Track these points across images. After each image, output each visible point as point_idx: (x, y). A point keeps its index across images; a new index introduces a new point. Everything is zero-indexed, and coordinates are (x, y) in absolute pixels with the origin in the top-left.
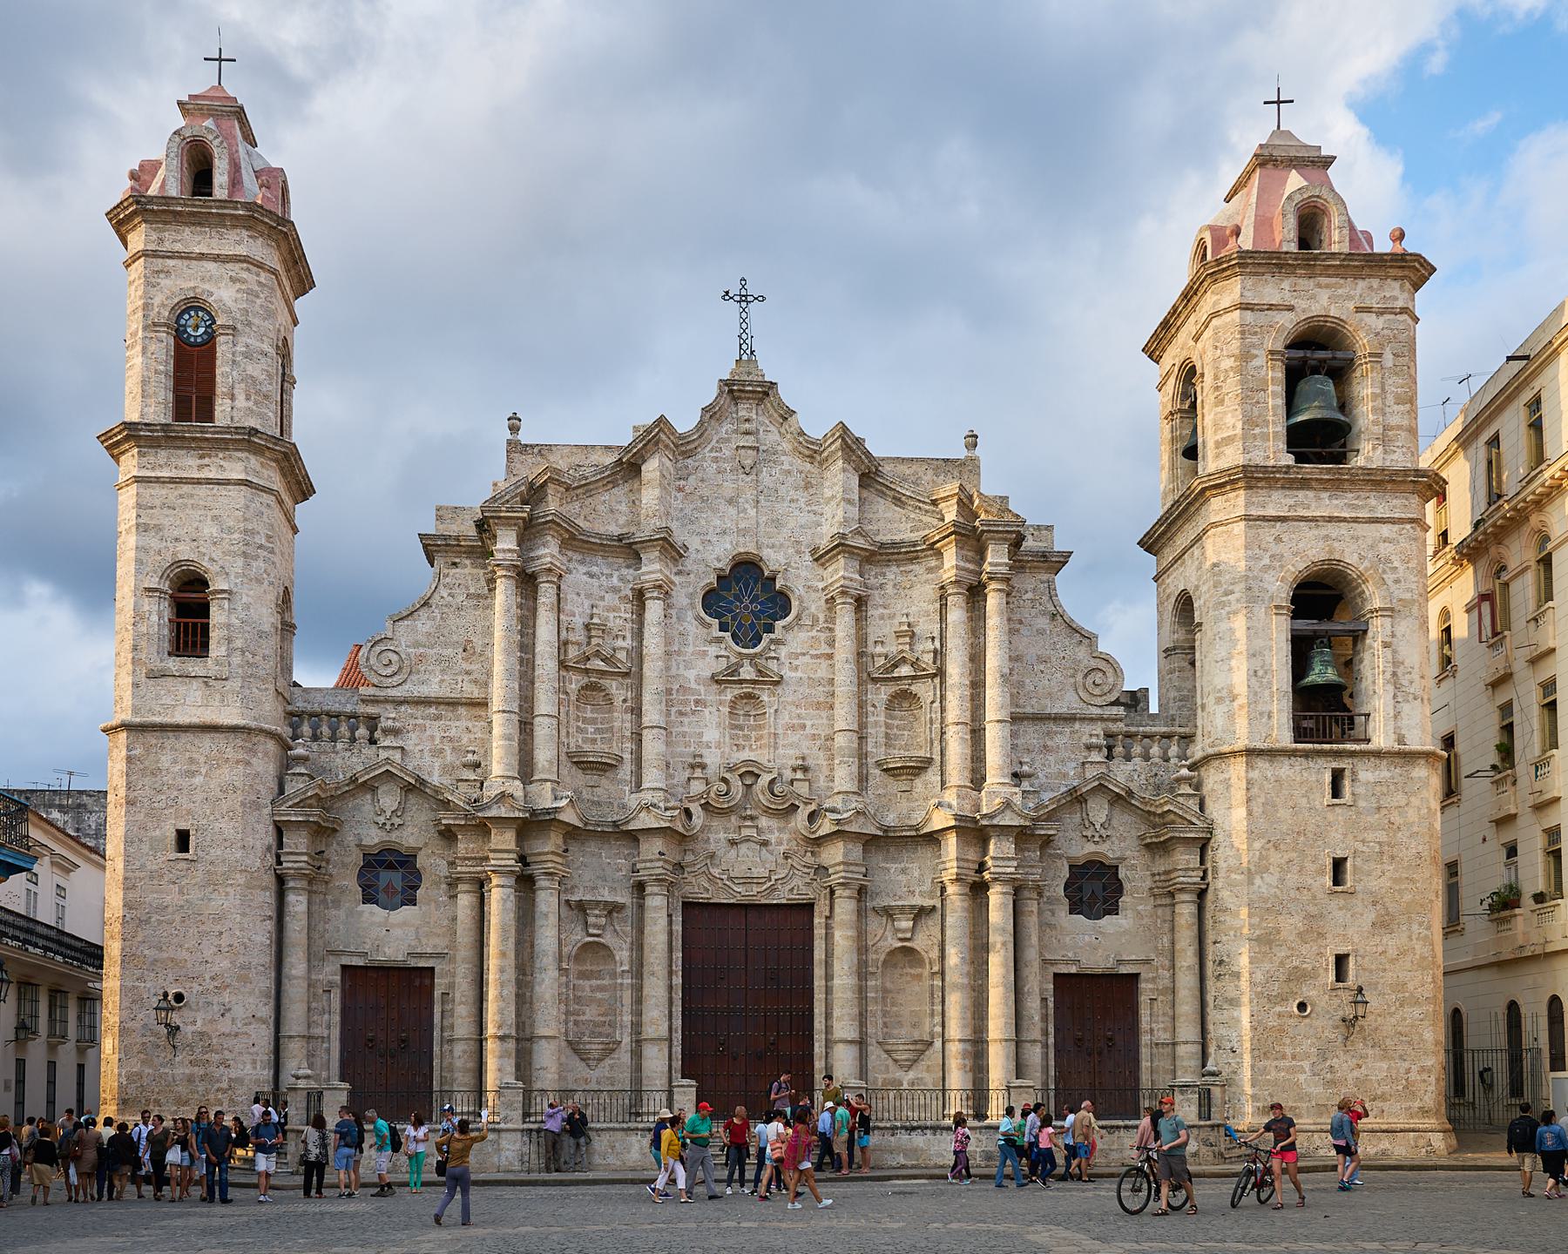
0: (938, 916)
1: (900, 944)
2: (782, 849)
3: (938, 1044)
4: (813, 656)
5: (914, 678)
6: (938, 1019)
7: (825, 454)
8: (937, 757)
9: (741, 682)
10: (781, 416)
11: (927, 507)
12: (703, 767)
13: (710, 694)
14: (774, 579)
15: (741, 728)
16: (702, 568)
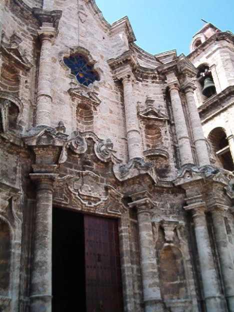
0: (183, 229)
1: (167, 244)
2: (104, 184)
3: (195, 302)
4: (110, 101)
5: (156, 120)
6: (192, 287)
7: (112, 30)
8: (171, 155)
9: (83, 98)
10: (95, 11)
11: (153, 61)
12: (64, 129)
13: (67, 98)
14: (93, 65)
15: (79, 122)
16: (63, 46)
